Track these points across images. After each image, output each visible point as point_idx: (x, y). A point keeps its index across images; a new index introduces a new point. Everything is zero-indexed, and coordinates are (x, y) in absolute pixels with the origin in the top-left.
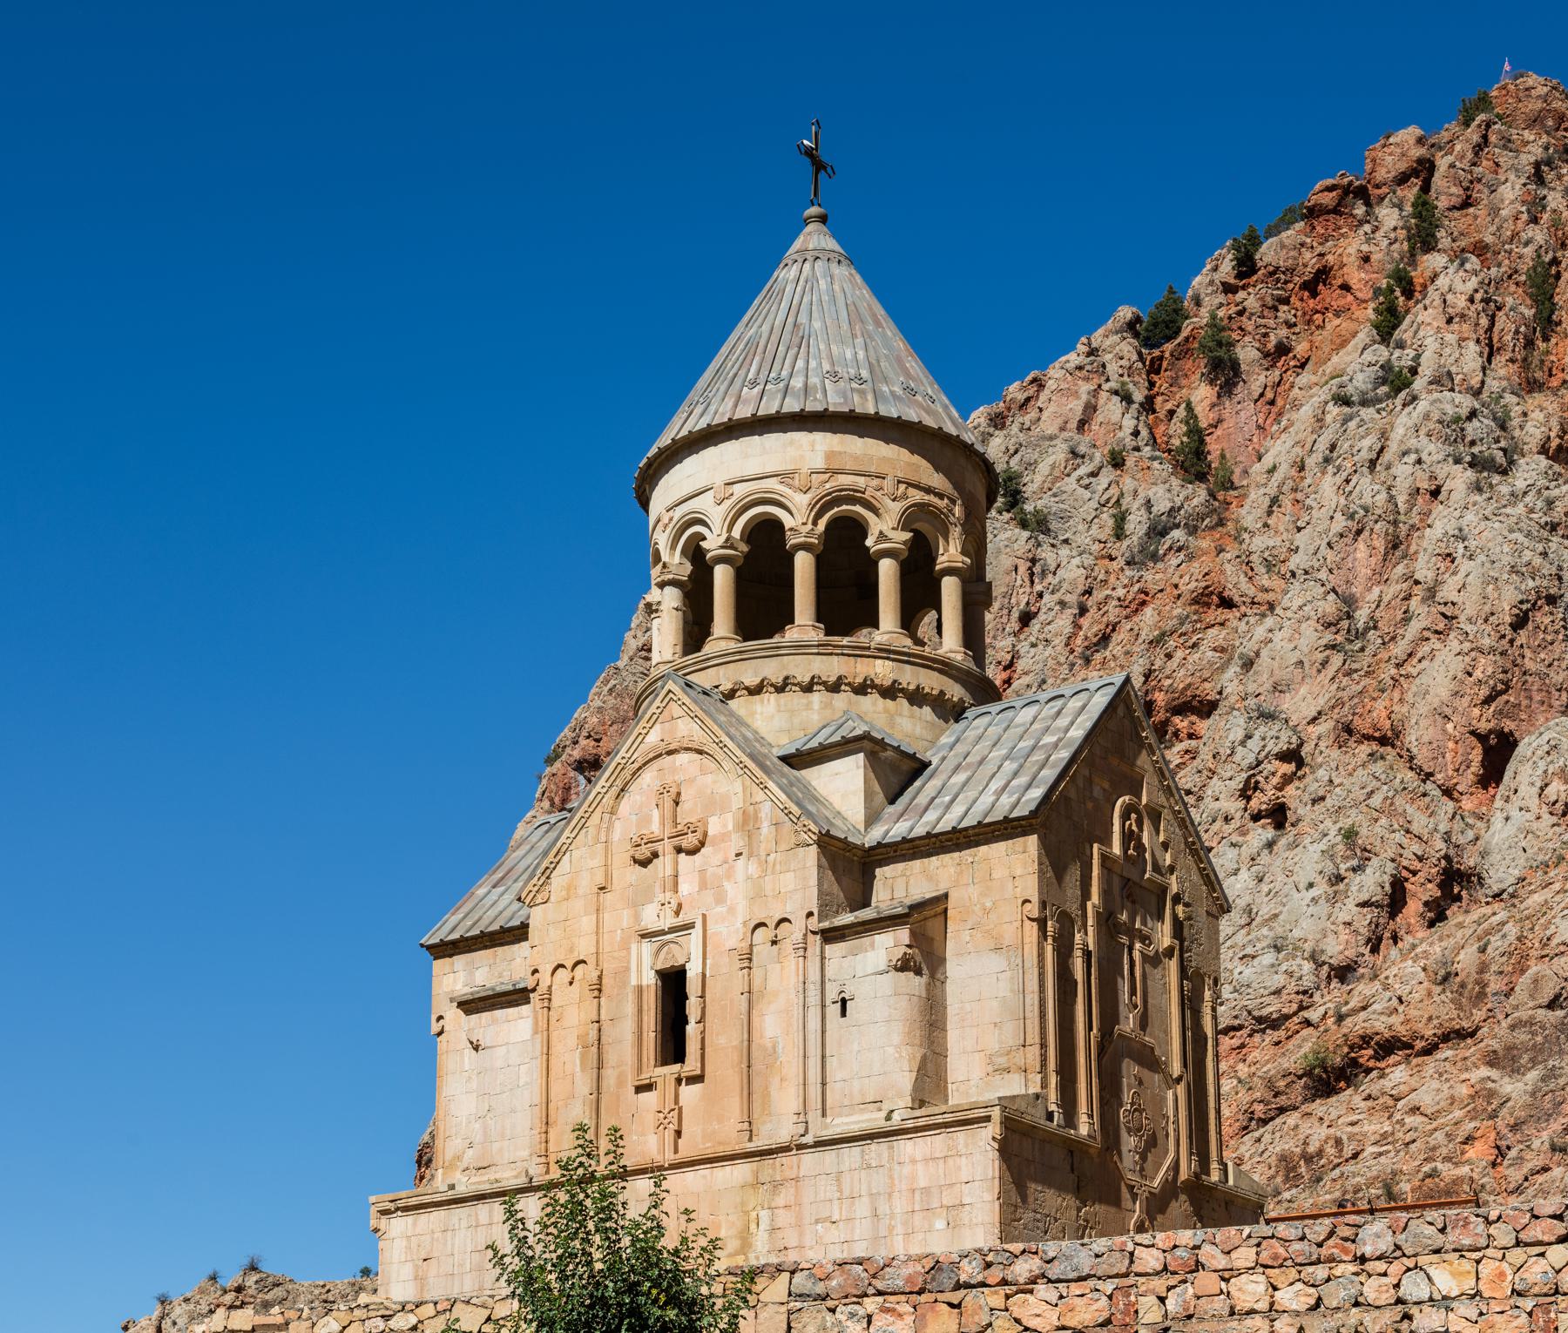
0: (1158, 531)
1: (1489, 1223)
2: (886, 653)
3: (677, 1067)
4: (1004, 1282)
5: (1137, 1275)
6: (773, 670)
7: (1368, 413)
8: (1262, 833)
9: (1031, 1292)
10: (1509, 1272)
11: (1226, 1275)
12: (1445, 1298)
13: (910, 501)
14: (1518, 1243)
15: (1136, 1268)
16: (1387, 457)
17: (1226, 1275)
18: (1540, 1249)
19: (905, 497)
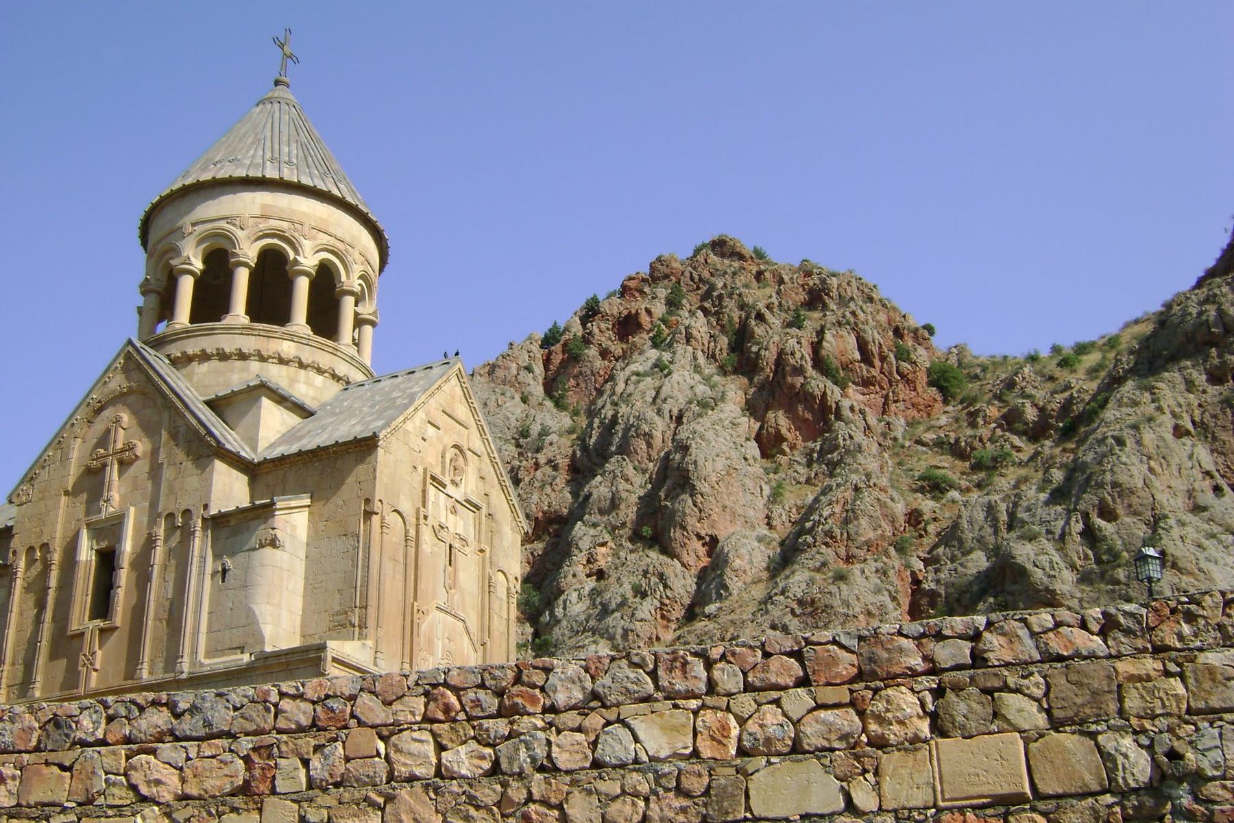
0: (544, 433)
1: (709, 665)
2: (292, 337)
3: (99, 623)
4: (128, 740)
5: (280, 732)
6: (208, 344)
7: (649, 379)
8: (591, 583)
9: (153, 752)
10: (733, 722)
11: (387, 732)
12: (651, 759)
13: (319, 242)
14: (748, 687)
15: (282, 724)
16: (659, 401)
17: (387, 732)
18: (775, 694)
19: (314, 238)
